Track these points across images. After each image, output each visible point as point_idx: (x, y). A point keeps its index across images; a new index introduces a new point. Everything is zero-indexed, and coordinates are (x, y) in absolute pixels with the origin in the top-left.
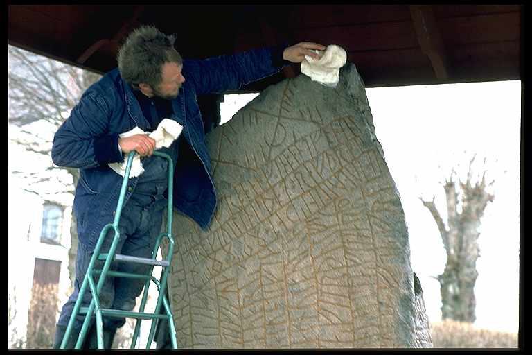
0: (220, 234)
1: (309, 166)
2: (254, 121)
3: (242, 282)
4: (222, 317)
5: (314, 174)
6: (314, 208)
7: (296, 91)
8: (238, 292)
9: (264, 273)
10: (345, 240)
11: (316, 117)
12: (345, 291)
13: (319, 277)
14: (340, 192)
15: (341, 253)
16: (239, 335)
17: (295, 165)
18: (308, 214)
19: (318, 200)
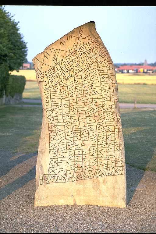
0: (61, 71)
1: (88, 51)
2: (71, 38)
3: (69, 84)
4: (62, 94)
5: (90, 54)
6: (90, 63)
7: (83, 30)
8: (67, 87)
9: (75, 81)
10: (100, 72)
11: (89, 38)
12: (100, 85)
13: (92, 82)
14: (98, 59)
15: (98, 76)
16: (68, 98)
17: (84, 52)
18: (88, 65)
19: (92, 62)
